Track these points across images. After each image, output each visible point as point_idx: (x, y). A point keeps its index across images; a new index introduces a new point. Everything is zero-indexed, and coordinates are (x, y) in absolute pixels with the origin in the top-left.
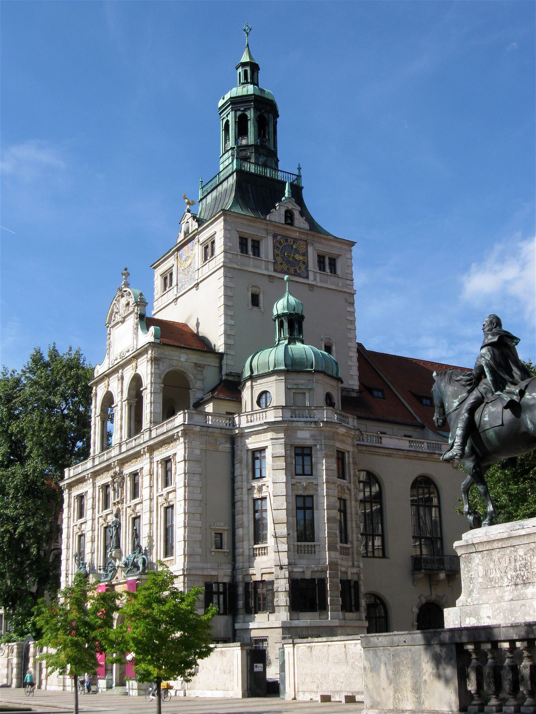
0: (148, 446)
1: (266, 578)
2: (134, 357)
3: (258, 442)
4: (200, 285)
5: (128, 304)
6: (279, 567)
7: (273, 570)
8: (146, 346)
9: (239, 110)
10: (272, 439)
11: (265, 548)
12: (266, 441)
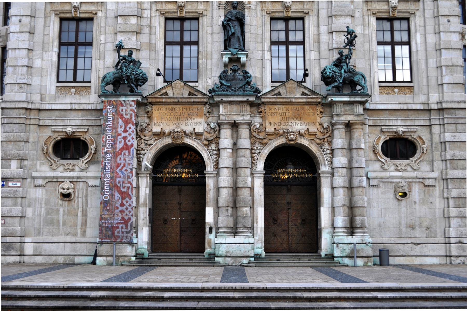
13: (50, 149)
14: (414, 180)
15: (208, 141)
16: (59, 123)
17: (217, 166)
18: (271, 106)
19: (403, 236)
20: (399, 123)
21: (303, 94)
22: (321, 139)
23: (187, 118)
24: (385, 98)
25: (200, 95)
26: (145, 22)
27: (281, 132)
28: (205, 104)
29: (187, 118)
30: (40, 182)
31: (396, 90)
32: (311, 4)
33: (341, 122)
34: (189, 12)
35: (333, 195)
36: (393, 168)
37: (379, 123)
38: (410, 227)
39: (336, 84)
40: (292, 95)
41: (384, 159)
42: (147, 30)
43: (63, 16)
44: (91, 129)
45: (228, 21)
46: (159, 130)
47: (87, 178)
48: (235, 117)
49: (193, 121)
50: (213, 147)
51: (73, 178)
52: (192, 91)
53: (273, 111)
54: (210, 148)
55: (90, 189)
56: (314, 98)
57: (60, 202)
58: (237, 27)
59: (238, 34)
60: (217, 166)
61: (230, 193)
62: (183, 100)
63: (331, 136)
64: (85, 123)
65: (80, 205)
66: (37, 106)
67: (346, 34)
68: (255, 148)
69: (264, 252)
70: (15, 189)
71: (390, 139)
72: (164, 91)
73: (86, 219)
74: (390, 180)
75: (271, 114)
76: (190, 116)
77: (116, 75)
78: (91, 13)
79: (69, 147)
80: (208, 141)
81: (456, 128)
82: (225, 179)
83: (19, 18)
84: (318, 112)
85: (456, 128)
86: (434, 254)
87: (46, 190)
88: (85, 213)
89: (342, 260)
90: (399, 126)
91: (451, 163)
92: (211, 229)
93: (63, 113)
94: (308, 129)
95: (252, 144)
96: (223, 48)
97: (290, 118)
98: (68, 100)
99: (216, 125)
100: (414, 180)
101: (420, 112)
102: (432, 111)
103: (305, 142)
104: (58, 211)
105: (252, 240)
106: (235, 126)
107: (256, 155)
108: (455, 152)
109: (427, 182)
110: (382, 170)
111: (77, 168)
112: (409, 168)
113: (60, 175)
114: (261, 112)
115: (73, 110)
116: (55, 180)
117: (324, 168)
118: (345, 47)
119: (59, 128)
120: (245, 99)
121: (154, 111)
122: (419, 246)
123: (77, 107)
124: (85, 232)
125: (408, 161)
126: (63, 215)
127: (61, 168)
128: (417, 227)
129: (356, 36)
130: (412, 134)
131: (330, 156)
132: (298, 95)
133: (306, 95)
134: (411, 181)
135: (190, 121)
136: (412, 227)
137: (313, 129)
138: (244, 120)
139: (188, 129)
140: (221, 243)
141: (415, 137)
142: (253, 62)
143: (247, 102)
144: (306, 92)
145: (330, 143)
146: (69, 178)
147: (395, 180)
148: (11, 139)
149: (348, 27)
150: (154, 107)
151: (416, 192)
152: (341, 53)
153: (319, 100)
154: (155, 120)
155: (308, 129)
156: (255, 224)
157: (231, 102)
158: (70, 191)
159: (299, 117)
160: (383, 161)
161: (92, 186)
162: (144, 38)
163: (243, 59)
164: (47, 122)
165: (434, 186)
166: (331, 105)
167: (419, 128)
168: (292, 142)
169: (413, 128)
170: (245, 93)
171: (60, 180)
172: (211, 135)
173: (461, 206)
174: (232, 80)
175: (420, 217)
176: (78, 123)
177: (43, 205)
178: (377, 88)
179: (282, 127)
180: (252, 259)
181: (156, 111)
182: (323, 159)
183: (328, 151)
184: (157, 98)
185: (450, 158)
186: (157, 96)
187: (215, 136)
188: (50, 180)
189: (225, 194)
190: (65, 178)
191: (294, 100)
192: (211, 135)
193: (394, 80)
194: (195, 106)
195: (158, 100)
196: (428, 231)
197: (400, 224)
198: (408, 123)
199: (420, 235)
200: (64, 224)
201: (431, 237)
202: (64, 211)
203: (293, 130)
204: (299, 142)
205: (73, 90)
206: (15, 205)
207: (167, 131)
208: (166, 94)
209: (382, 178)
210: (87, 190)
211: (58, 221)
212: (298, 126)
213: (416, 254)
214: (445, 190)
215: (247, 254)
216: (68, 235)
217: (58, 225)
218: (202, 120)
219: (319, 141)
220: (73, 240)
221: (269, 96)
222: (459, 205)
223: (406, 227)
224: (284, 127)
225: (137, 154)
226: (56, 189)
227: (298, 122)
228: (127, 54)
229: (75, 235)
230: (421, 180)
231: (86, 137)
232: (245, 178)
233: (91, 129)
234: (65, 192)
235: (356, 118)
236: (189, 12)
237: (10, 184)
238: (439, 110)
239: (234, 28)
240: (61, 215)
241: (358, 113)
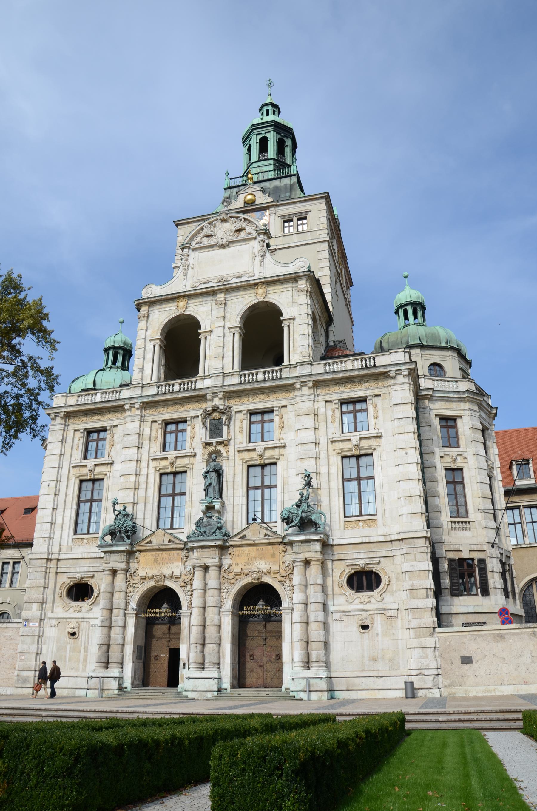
0: (313, 381)
1: (476, 556)
2: (263, 283)
3: (451, 409)
4: (278, 251)
5: (239, 231)
6: (491, 545)
7: (485, 548)
8: (302, 274)
9: (280, 134)
10: (470, 409)
11: (466, 522)
12: (464, 410)
13: (65, 593)
14: (376, 612)
15: (185, 583)
16: (72, 570)
17: (190, 606)
18: (238, 548)
19: (366, 669)
20: (362, 555)
21: (266, 535)
22: (283, 577)
23: (167, 563)
24: (350, 533)
25: (177, 542)
26: (142, 479)
27: (246, 571)
28: (182, 549)
29: (167, 563)
30: (54, 622)
31: (361, 524)
32: (281, 450)
33: (298, 560)
34: (178, 467)
38: (373, 660)
39: (293, 524)
40: (256, 537)
42: (143, 486)
43: (81, 478)
44: (96, 574)
46: (144, 575)
47: (89, 618)
48: (206, 559)
49: (172, 565)
50: (188, 588)
51: (79, 618)
52: (172, 539)
53: (240, 553)
54: (185, 589)
55: (91, 628)
56: (275, 539)
57: (68, 640)
58: (213, 477)
60: (190, 606)
61: (199, 631)
62: (164, 547)
63: (292, 574)
64: (91, 569)
65: (83, 643)
66: (55, 556)
67: (303, 476)
68: (224, 588)
69: (229, 687)
70: (33, 629)
71: (355, 572)
72: (149, 540)
73: (87, 655)
74: (352, 613)
75: (238, 556)
76: (170, 560)
77: (112, 528)
78: (102, 474)
79: (80, 591)
80: (185, 583)
81: (415, 557)
82: (196, 618)
83: (48, 483)
84: (281, 551)
85: (415, 557)
86: (396, 687)
87: (58, 629)
88: (86, 651)
89: (298, 694)
90: (361, 559)
91: (410, 593)
92: (184, 665)
93: (75, 561)
94: (270, 568)
97: (255, 558)
98: (81, 549)
99: (191, 568)
100: (376, 612)
101: (382, 544)
102: (393, 542)
103: (267, 579)
104: (66, 648)
106: (206, 568)
107: (224, 594)
108: (414, 582)
109: (389, 613)
110: (347, 603)
111: (83, 609)
114: (230, 554)
115: (85, 558)
116: (65, 620)
117: (285, 604)
118: (304, 489)
119: (71, 575)
120: (212, 543)
121: (141, 558)
122: (382, 679)
123: (85, 556)
124: (86, 667)
125: (372, 593)
126: (70, 652)
127: (72, 610)
128: (380, 660)
129: (311, 478)
130: (375, 566)
131: (290, 592)
132: (262, 536)
133: (269, 536)
135: (170, 565)
136: (375, 660)
137: (275, 568)
138: (213, 562)
139: (167, 572)
140: (190, 679)
141: (378, 569)
142: (229, 507)
143: (216, 546)
144: (269, 533)
145: (291, 580)
146: (76, 618)
147: (357, 613)
148: (34, 585)
149: (306, 470)
150: (141, 554)
152: (302, 495)
153: (280, 540)
154: (142, 565)
155: (270, 568)
156: (222, 660)
157: (202, 547)
158: (75, 630)
159: (262, 557)
160: (347, 594)
161: (93, 626)
162: (141, 493)
163: (217, 506)
164: (63, 570)
165: (396, 617)
166: (291, 543)
167: (382, 559)
168: (256, 581)
169: (376, 561)
171: (68, 620)
172: (187, 577)
173: (422, 636)
174: (207, 526)
175: (383, 650)
176: (86, 569)
177: (55, 643)
178: (342, 523)
179: (247, 567)
180: (216, 693)
181: (142, 557)
182: (285, 596)
183: (289, 588)
184: (142, 546)
185: (409, 588)
186: (143, 544)
187: (190, 578)
188: (61, 620)
189: (195, 631)
190: (72, 618)
191: (257, 542)
192: (187, 577)
193: (361, 515)
194: (174, 552)
195: (144, 548)
196: (390, 664)
197: (363, 657)
199: (383, 668)
200: (70, 660)
201: (394, 669)
202: (70, 648)
203: (256, 570)
204: (262, 580)
205: (85, 541)
206: (33, 643)
207: (150, 575)
208: (150, 542)
209: (344, 612)
210: (89, 629)
211: (65, 657)
212: (263, 566)
213: (378, 688)
215: (211, 689)
216: (72, 669)
217: (65, 661)
218: (178, 564)
219: (281, 579)
221: (235, 539)
222: (420, 635)
223: (369, 660)
224: (249, 567)
225: (126, 596)
226: (65, 629)
227: (262, 562)
228: (122, 509)
229: (78, 670)
230: (382, 612)
231: (91, 582)
232: (211, 616)
233: (96, 574)
234: (72, 631)
235: (313, 555)
236: (178, 467)
237: (31, 624)
238: (399, 540)
239: (211, 478)
240: (68, 652)
241: (314, 550)
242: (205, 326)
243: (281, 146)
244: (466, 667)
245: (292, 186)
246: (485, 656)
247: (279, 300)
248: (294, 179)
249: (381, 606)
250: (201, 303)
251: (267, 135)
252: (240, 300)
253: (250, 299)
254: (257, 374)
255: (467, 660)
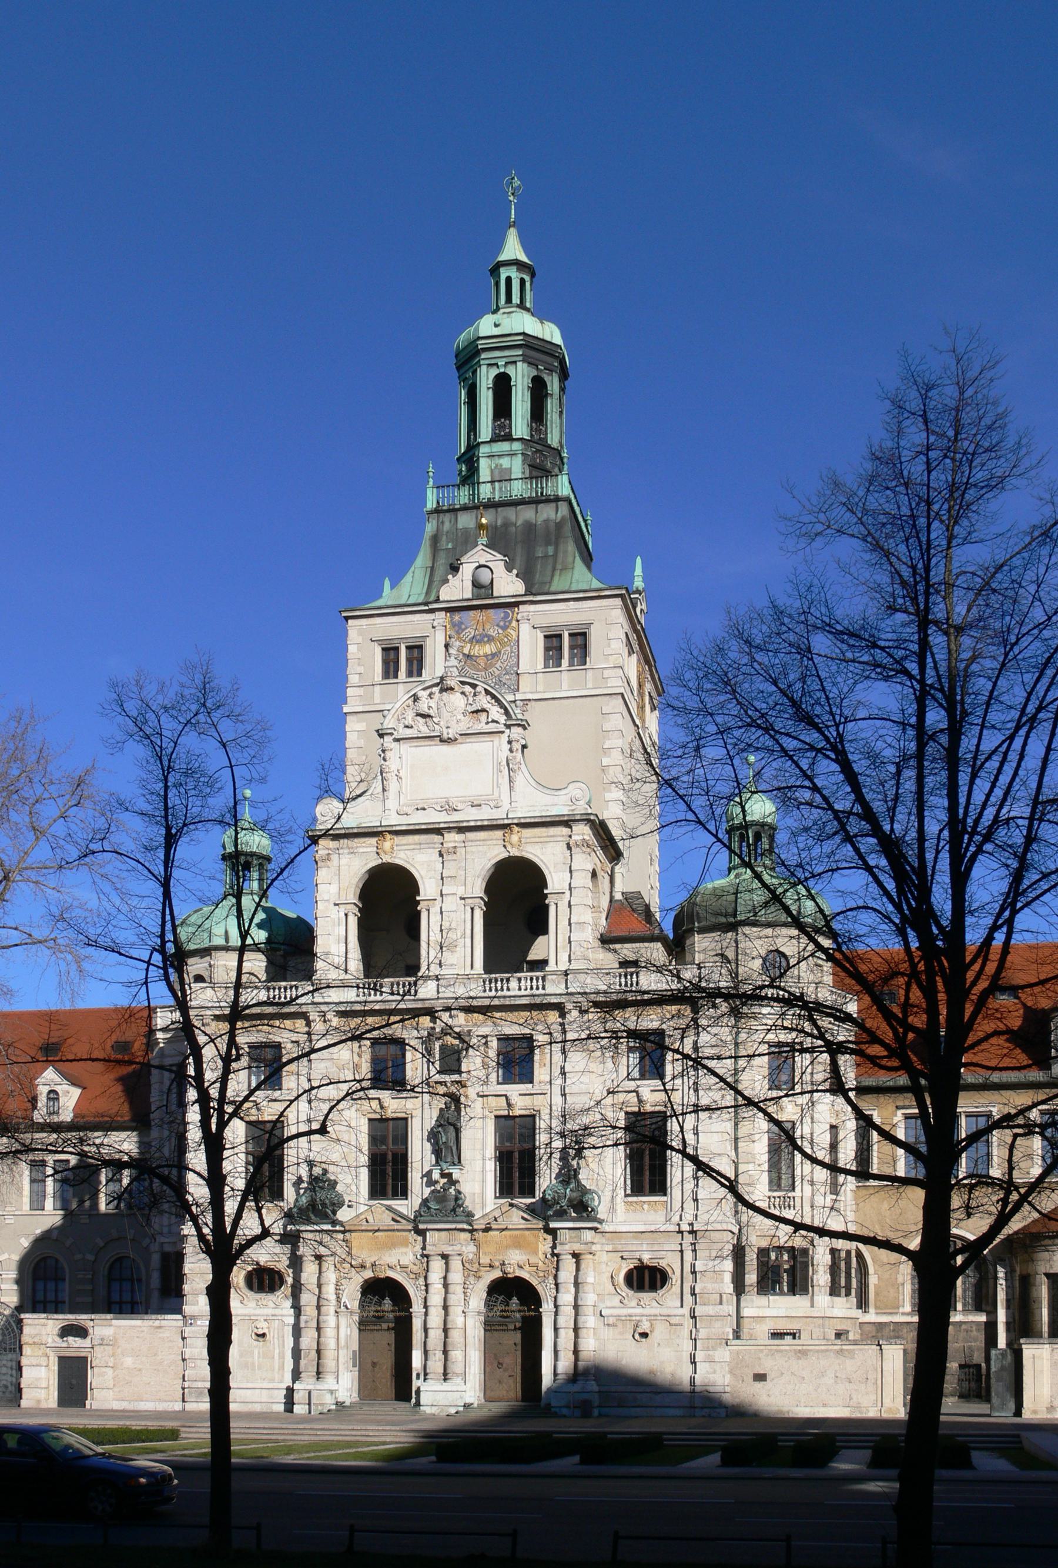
31: (646, 1206)
35: (556, 1336)
36: (634, 1303)
37: (620, 1248)
41: (625, 1291)
45: (439, 1126)
59: (452, 1143)
76: (393, 1246)
82: (435, 1319)
92: (418, 1375)
95: (466, 1277)
96: (434, 1162)
97: (508, 1247)
105: (463, 1388)
109: (673, 1320)
112: (655, 1304)
113: (252, 1312)
134: (652, 1319)
139: (393, 1261)
151: (659, 1333)
159: (517, 1244)
160: (624, 1294)
170: (458, 1218)
180: (461, 1409)
198: (656, 1248)
200: (259, 1369)
211: (253, 1364)
214: (694, 1330)
220: (271, 1386)
227: (517, 1252)
229: (272, 1381)
234: (260, 1332)
237: (199, 1323)
242: (427, 889)
243: (538, 390)
244: (759, 1385)
245: (559, 526)
246: (782, 1374)
247: (542, 857)
248: (563, 510)
249: (665, 1311)
250: (418, 847)
251: (510, 371)
252: (480, 848)
253: (496, 852)
254: (508, 980)
255: (760, 1377)
